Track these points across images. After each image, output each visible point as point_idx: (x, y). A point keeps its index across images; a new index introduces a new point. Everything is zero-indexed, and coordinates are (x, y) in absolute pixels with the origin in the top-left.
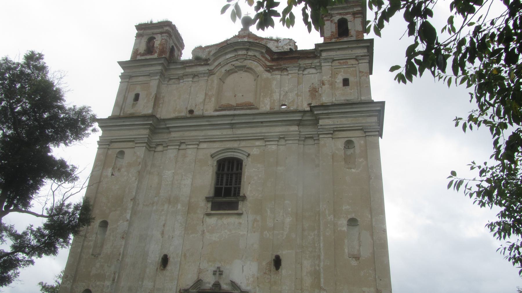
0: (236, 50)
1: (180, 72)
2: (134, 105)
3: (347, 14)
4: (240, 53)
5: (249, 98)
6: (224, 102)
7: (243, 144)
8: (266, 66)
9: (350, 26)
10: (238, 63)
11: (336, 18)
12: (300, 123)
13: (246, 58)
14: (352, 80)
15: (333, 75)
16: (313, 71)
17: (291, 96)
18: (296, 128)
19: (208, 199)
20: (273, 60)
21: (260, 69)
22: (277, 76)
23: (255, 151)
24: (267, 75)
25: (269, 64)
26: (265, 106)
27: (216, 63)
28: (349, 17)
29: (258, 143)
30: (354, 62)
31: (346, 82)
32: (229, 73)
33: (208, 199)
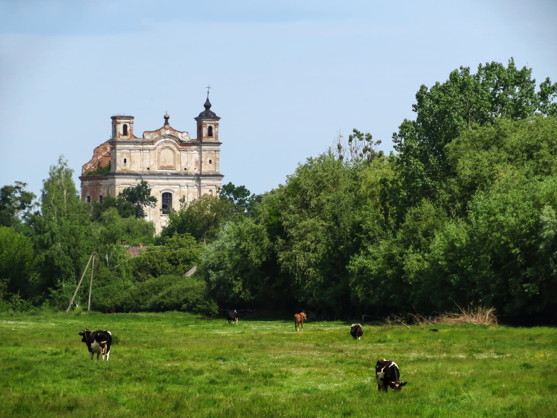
0: (165, 138)
1: (141, 146)
2: (125, 165)
3: (212, 124)
4: (167, 139)
5: (171, 164)
6: (161, 164)
7: (172, 186)
8: (178, 148)
9: (213, 131)
10: (166, 145)
11: (208, 125)
12: (193, 179)
13: (169, 142)
14: (213, 161)
15: (206, 158)
16: (196, 152)
17: (188, 164)
18: (191, 181)
19: (161, 210)
20: (181, 145)
21: (175, 149)
22: (184, 154)
23: (176, 190)
24: (178, 152)
25: (179, 147)
26: (178, 170)
27: (157, 143)
28: (213, 126)
29: (178, 186)
30: (213, 152)
31: (210, 161)
32: (163, 149)
33: (161, 210)
